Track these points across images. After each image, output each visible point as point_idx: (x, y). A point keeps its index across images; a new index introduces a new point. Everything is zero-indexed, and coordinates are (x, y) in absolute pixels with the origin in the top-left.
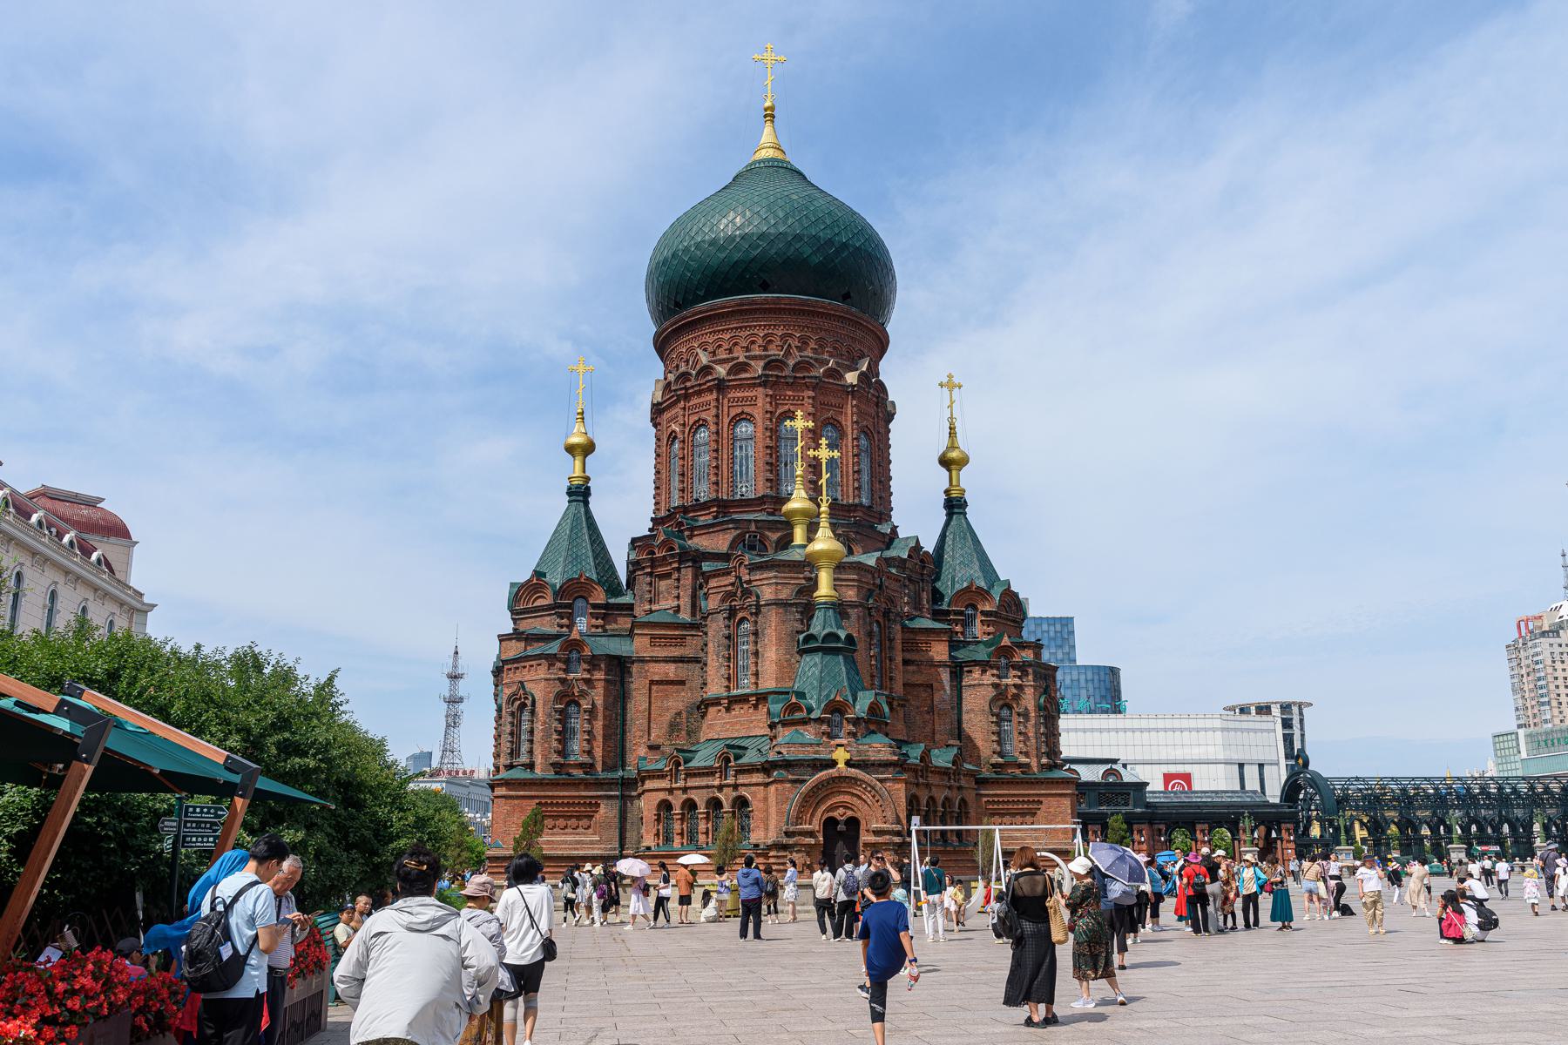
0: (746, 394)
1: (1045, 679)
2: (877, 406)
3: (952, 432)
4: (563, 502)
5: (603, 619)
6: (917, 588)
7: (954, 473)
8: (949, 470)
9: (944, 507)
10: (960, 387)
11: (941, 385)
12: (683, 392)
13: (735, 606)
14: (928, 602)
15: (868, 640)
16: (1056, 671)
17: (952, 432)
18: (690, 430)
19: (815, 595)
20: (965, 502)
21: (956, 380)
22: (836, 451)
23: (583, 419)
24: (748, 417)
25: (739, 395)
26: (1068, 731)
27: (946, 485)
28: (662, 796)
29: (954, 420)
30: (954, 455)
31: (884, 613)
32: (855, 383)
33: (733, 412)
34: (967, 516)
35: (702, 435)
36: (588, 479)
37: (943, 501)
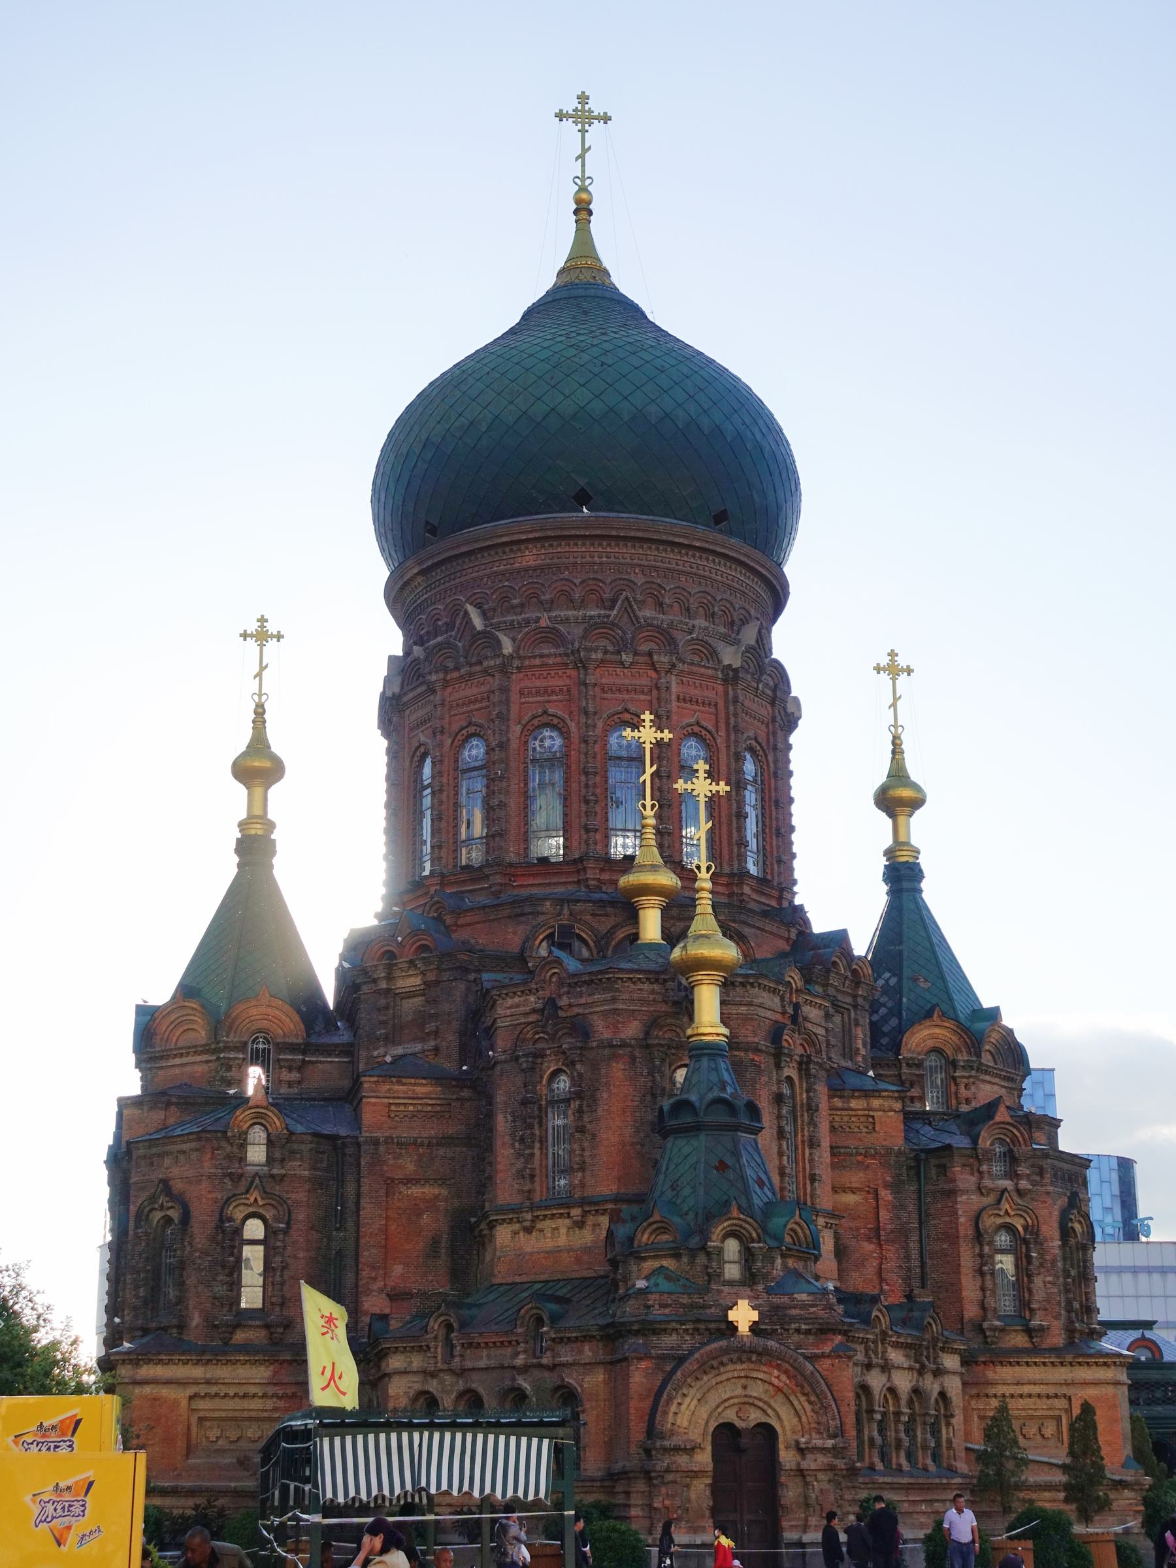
1: (1070, 1180)
2: (773, 704)
4: (227, 868)
5: (300, 1069)
6: (846, 1020)
7: (901, 819)
8: (892, 814)
9: (884, 880)
11: (878, 669)
12: (441, 675)
14: (864, 1045)
15: (776, 1111)
16: (1088, 1167)
18: (452, 743)
19: (689, 1032)
21: (902, 661)
24: (555, 721)
26: (1108, 1270)
27: (888, 842)
28: (415, 1384)
29: (900, 729)
31: (800, 1063)
32: (737, 664)
35: (474, 752)
37: (882, 870)
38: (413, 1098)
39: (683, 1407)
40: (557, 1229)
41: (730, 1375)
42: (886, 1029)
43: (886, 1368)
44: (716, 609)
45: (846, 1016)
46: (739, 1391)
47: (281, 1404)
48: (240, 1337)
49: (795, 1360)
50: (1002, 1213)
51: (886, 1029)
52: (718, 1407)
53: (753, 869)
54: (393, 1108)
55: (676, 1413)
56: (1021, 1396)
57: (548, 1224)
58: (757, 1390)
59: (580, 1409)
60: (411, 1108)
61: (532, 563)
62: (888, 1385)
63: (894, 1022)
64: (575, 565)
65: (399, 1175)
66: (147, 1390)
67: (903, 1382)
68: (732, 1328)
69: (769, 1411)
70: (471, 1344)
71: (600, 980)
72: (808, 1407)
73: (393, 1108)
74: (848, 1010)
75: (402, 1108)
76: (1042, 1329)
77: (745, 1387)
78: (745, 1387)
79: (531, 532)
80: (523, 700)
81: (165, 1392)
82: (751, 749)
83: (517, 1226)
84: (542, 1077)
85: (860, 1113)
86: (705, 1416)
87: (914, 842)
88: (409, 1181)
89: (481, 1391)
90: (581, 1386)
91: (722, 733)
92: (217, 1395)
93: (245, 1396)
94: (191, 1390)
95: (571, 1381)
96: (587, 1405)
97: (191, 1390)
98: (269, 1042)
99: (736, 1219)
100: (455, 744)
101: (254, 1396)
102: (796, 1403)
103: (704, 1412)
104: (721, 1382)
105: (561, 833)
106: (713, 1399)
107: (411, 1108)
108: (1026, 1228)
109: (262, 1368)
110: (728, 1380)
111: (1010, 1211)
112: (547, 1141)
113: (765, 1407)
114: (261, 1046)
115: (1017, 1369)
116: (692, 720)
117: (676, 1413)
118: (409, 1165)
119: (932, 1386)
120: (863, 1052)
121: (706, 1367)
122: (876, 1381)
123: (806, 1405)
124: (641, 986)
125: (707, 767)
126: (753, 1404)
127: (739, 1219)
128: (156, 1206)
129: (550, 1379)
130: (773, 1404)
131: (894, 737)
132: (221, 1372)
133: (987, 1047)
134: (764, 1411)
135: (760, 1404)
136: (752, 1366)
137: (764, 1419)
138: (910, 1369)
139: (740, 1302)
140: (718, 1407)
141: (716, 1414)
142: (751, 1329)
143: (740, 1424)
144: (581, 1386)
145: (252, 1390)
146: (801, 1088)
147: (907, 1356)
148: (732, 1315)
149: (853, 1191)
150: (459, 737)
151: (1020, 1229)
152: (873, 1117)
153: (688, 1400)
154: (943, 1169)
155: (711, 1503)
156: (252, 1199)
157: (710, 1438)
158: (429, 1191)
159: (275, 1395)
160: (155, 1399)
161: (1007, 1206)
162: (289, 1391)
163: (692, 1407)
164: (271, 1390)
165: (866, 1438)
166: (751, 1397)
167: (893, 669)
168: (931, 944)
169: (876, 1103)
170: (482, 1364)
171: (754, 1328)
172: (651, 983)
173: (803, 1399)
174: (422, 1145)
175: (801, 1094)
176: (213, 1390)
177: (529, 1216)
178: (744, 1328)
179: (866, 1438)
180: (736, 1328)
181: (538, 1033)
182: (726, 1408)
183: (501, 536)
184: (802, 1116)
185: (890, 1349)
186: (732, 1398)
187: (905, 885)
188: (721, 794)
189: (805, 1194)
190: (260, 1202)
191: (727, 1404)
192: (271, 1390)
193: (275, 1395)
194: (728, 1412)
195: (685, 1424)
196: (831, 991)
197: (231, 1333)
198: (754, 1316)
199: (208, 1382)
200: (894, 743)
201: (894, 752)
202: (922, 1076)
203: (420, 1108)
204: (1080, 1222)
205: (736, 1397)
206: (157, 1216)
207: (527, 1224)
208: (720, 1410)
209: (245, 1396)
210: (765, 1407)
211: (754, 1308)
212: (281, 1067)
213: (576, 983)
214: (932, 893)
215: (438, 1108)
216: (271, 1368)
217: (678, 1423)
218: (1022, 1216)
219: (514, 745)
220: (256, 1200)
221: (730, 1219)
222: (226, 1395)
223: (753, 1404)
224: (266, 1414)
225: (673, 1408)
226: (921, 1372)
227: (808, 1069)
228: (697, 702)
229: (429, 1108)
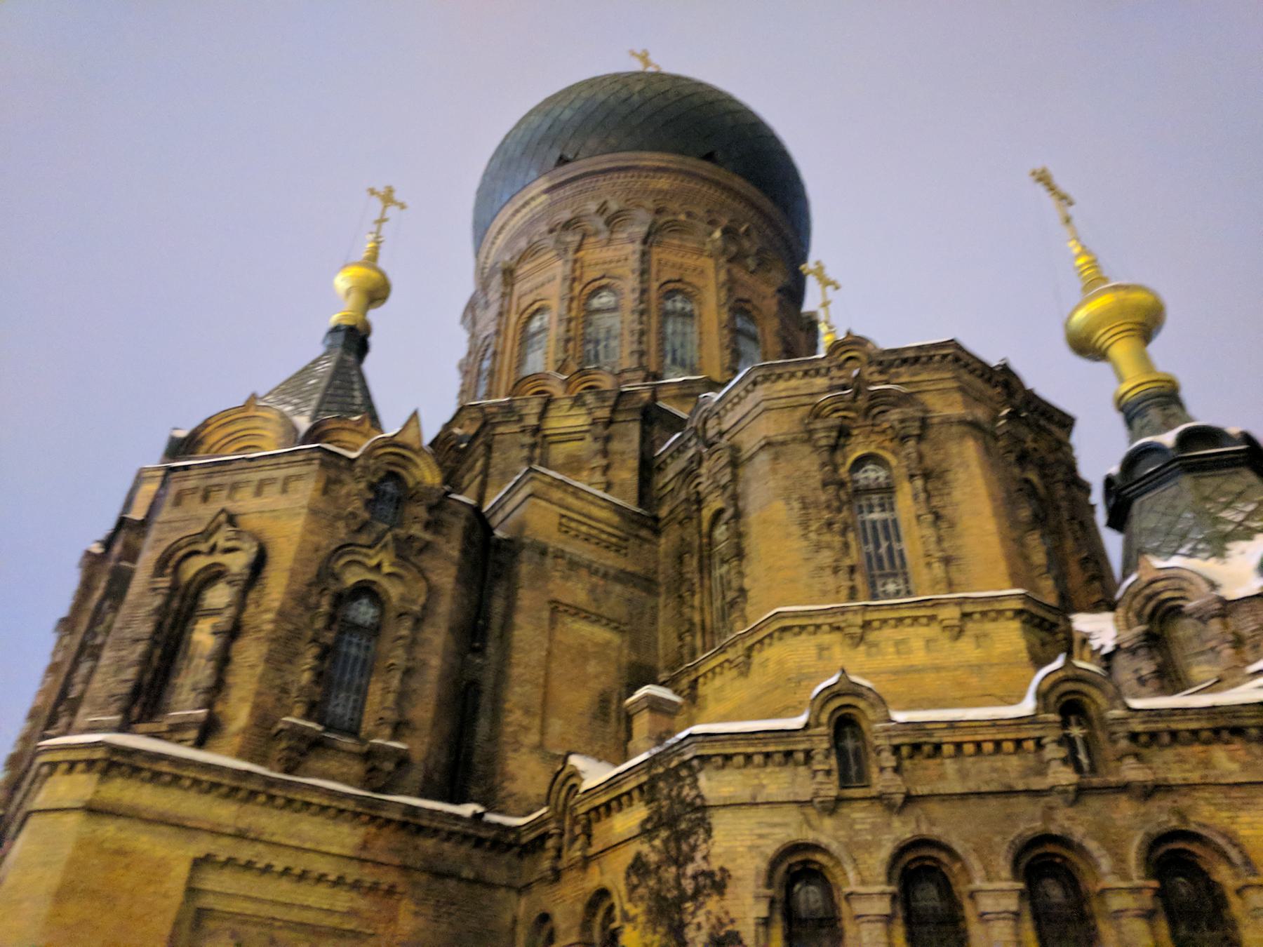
47: (362, 903)
65: (567, 599)
81: (146, 842)
88: (577, 612)
92: (249, 866)
93: (303, 876)
94: (202, 846)
97: (202, 846)
101: (321, 878)
118: (576, 591)
145: (320, 866)
156: (374, 562)
158: (601, 634)
160: (120, 852)
164: (353, 872)
174: (596, 572)
176: (245, 853)
190: (387, 568)
192: (353, 872)
193: (356, 885)
197: (303, 754)
199: (240, 835)
209: (303, 876)
216: (362, 831)
222: (268, 869)
224: (334, 921)
229: (604, 536)
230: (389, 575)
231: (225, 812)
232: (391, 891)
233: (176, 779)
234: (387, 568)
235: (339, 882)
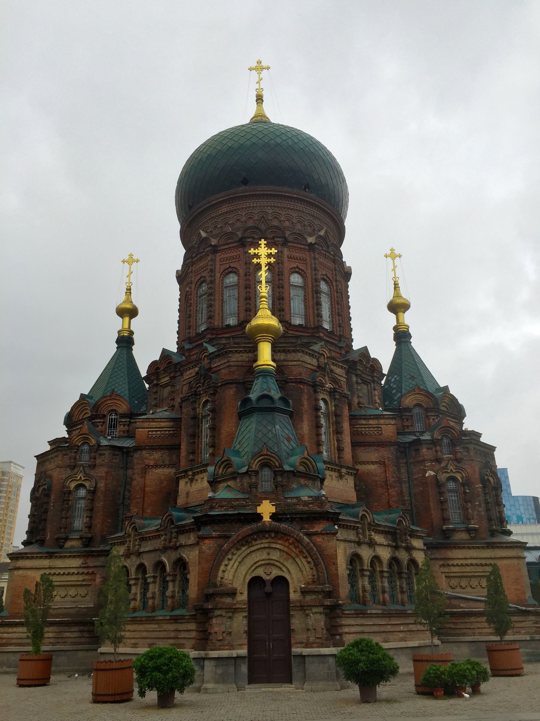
0: (233, 254)
3: (396, 286)
6: (370, 387)
9: (394, 340)
10: (400, 256)
11: (386, 256)
12: (190, 260)
13: (200, 391)
17: (396, 286)
18: (195, 286)
19: (254, 365)
20: (410, 334)
21: (397, 252)
22: (273, 249)
23: (131, 293)
25: (227, 256)
27: (395, 323)
30: (399, 301)
33: (223, 268)
34: (412, 344)
35: (204, 288)
36: (132, 333)
38: (159, 428)
39: (229, 567)
40: (203, 478)
41: (259, 546)
42: (396, 398)
43: (372, 544)
44: (306, 223)
45: (369, 386)
46: (265, 556)
47: (86, 577)
48: (69, 544)
49: (298, 535)
50: (449, 471)
51: (396, 398)
52: (252, 566)
53: (326, 326)
54: (150, 433)
55: (224, 571)
56: (467, 565)
57: (201, 476)
58: (275, 556)
59: (187, 572)
60: (159, 433)
61: (226, 210)
62: (374, 554)
63: (399, 395)
64: (243, 208)
66: (21, 572)
67: (385, 554)
68: (259, 517)
69: (284, 568)
70: (143, 538)
71: (222, 353)
72: (307, 566)
73: (150, 433)
74: (370, 383)
75: (154, 433)
76: (475, 530)
77: (269, 554)
78: (269, 554)
79: (223, 197)
80: (221, 263)
82: (324, 280)
83: (187, 480)
84: (199, 405)
85: (374, 426)
86: (244, 573)
87: (406, 323)
88: (156, 466)
89: (146, 564)
90: (188, 558)
91: (309, 271)
93: (69, 574)
95: (184, 556)
96: (191, 569)
98: (117, 415)
99: (265, 455)
100: (197, 286)
101: (73, 574)
102: (299, 562)
103: (243, 570)
104: (254, 551)
105: (237, 315)
106: (249, 561)
107: (159, 433)
108: (462, 478)
109: (78, 560)
110: (258, 549)
111: (453, 470)
112: (202, 435)
113: (281, 566)
114: (113, 417)
115: (464, 551)
116: (295, 266)
117: (224, 571)
119: (403, 556)
120: (378, 401)
121: (245, 541)
122: (366, 553)
123: (305, 563)
124: (242, 354)
125: (266, 242)
126: (273, 565)
127: (268, 455)
128: (40, 484)
129: (174, 556)
130: (285, 563)
131: (395, 282)
132: (59, 563)
133: (444, 404)
134: (281, 569)
135: (278, 564)
136: (273, 540)
137: (280, 573)
138: (388, 546)
139: (264, 501)
140: (252, 566)
141: (251, 571)
142: (271, 517)
143: (266, 577)
144: (188, 558)
145: (72, 571)
146: (331, 405)
147: (386, 538)
148: (259, 510)
149: (373, 463)
150: (198, 284)
151: (459, 479)
152: (381, 427)
153: (232, 562)
154: (417, 450)
155: (246, 629)
156: (79, 477)
157: (246, 586)
159: (83, 573)
161: (452, 467)
162: (90, 571)
163: (235, 566)
164: (81, 571)
165: (360, 586)
166: (272, 559)
167: (393, 255)
168: (415, 362)
169: (382, 421)
170: (147, 549)
171: (273, 517)
172: (248, 353)
173: (304, 560)
175: (332, 407)
177: (190, 473)
178: (266, 518)
179: (360, 586)
180: (262, 518)
181: (198, 384)
182: (257, 567)
183: (212, 201)
184: (332, 418)
185: (373, 534)
186: (260, 560)
187: (403, 340)
188: (273, 254)
189: (335, 457)
190: (83, 479)
191: (257, 565)
192: (81, 571)
193: (83, 573)
194: (259, 569)
195: (231, 577)
196: (359, 372)
197: (64, 543)
198: (273, 510)
199: (50, 568)
200: (395, 284)
201: (395, 288)
202: (412, 416)
203: (163, 432)
204: (491, 476)
205: (263, 560)
206: (41, 489)
207: (190, 477)
208: (253, 568)
209: (69, 574)
210: (281, 566)
211: (273, 505)
212: (121, 425)
213: (213, 357)
214: (415, 343)
215: (171, 432)
217: (225, 577)
218: (460, 472)
219: (217, 281)
220: (81, 477)
221: (262, 455)
223: (273, 565)
224: (79, 583)
225: (222, 568)
226: (396, 548)
227: (334, 395)
228: (297, 258)
229: (167, 432)
230: (84, 480)
231: (46, 563)
232: (93, 573)
233: (32, 558)
234: (83, 479)
235: (78, 573)
